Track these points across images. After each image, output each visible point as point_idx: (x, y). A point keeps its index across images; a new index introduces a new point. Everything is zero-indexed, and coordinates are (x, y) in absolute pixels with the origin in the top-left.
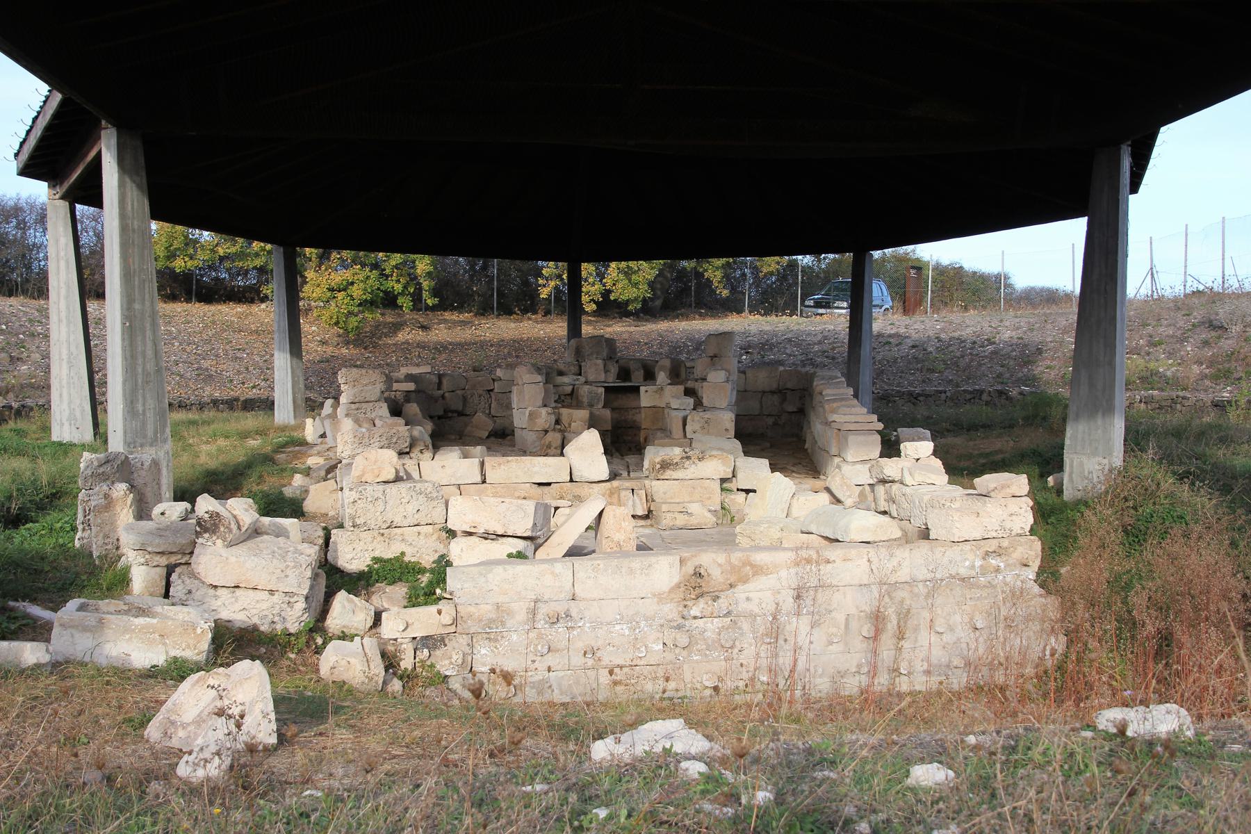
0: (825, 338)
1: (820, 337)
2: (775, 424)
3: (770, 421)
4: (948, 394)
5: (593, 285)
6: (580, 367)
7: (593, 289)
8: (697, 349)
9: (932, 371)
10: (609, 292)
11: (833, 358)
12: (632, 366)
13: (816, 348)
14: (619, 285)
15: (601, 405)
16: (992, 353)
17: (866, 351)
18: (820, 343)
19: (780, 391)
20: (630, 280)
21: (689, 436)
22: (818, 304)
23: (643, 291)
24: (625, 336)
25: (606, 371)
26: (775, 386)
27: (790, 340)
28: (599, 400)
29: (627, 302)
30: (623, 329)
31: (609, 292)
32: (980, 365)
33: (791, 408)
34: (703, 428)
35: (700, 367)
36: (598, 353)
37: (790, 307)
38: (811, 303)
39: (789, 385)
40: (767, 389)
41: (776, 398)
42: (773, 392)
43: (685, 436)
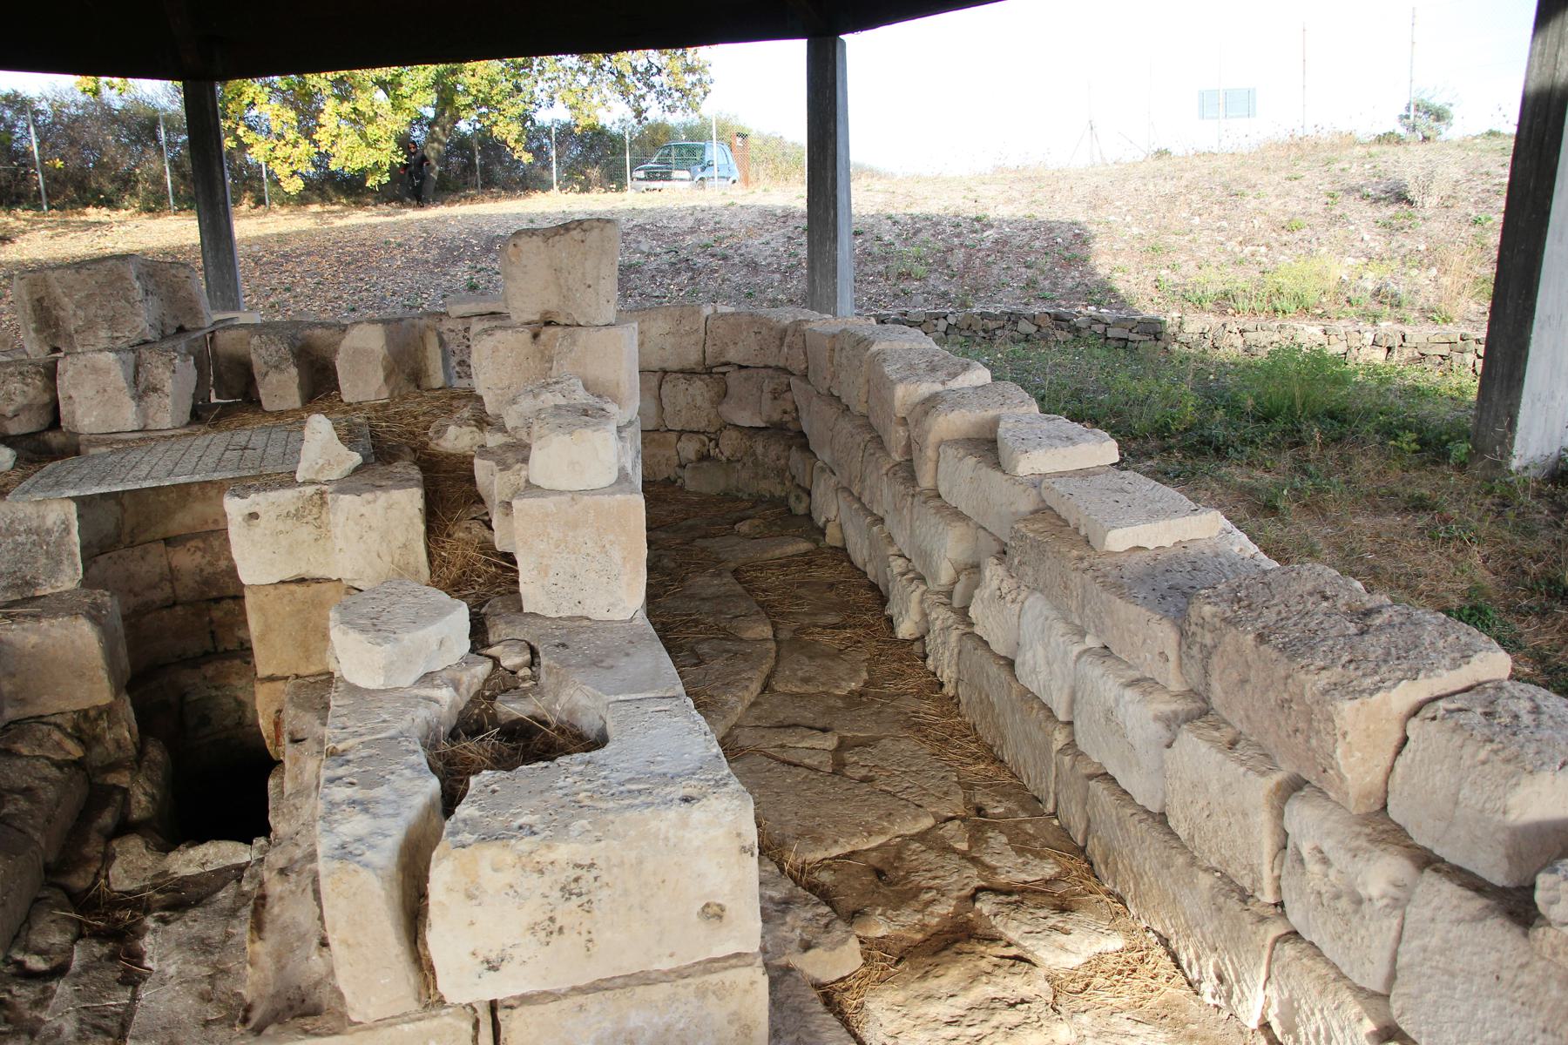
0: (699, 221)
1: (690, 222)
2: (704, 457)
3: (689, 448)
4: (952, 320)
5: (295, 145)
6: (50, 373)
7: (296, 152)
8: (489, 251)
9: (908, 276)
10: (326, 156)
11: (725, 258)
12: (261, 354)
13: (689, 240)
14: (343, 144)
15: (69, 578)
16: (996, 242)
17: (846, 249)
18: (692, 231)
19: (709, 371)
20: (363, 136)
21: (461, 982)
22: (651, 176)
23: (388, 155)
24: (364, 234)
25: (142, 389)
26: (692, 357)
27: (642, 228)
28: (56, 561)
29: (363, 173)
30: (382, 219)
31: (326, 156)
32: (988, 265)
33: (746, 418)
34: (552, 929)
35: (494, 366)
36: (113, 322)
37: (615, 178)
38: (641, 174)
39: (733, 355)
40: (672, 364)
41: (699, 391)
42: (688, 373)
43: (429, 995)
